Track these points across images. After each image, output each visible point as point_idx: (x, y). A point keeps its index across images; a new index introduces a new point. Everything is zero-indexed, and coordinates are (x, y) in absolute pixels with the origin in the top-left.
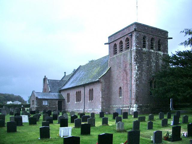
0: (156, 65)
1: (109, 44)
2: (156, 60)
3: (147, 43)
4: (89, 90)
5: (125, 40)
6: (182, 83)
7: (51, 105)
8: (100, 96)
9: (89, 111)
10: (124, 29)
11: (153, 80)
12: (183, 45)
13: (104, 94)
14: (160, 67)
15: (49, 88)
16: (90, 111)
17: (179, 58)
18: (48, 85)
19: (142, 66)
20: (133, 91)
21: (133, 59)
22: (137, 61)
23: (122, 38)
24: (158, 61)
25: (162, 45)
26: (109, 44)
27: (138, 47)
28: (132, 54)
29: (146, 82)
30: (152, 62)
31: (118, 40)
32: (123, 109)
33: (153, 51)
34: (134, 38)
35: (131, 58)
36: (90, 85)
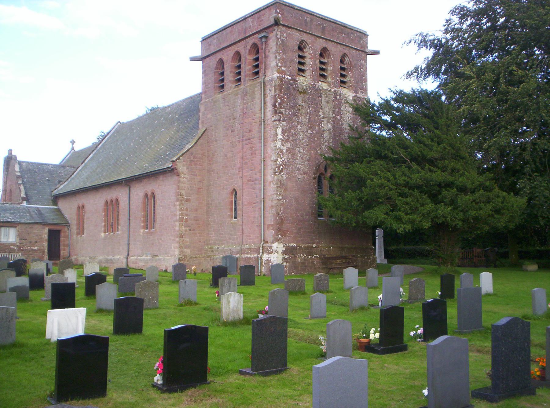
0: (333, 127)
1: (202, 59)
2: (334, 112)
3: (308, 61)
4: (142, 195)
5: (247, 51)
6: (408, 183)
7: (24, 242)
8: (175, 215)
9: (141, 260)
10: (245, 19)
11: (326, 169)
12: (414, 78)
13: (187, 210)
14: (346, 135)
15: (22, 187)
16: (146, 261)
17: (398, 109)
18: (18, 177)
19: (294, 127)
20: (269, 203)
21: (269, 108)
22: (281, 113)
23: (239, 44)
24: (338, 117)
25: (351, 70)
26: (202, 59)
27: (283, 72)
28: (268, 91)
29: (306, 177)
30: (324, 118)
31: (229, 49)
32: (243, 256)
33: (324, 86)
34: (272, 44)
35: (265, 103)
36: (146, 180)
